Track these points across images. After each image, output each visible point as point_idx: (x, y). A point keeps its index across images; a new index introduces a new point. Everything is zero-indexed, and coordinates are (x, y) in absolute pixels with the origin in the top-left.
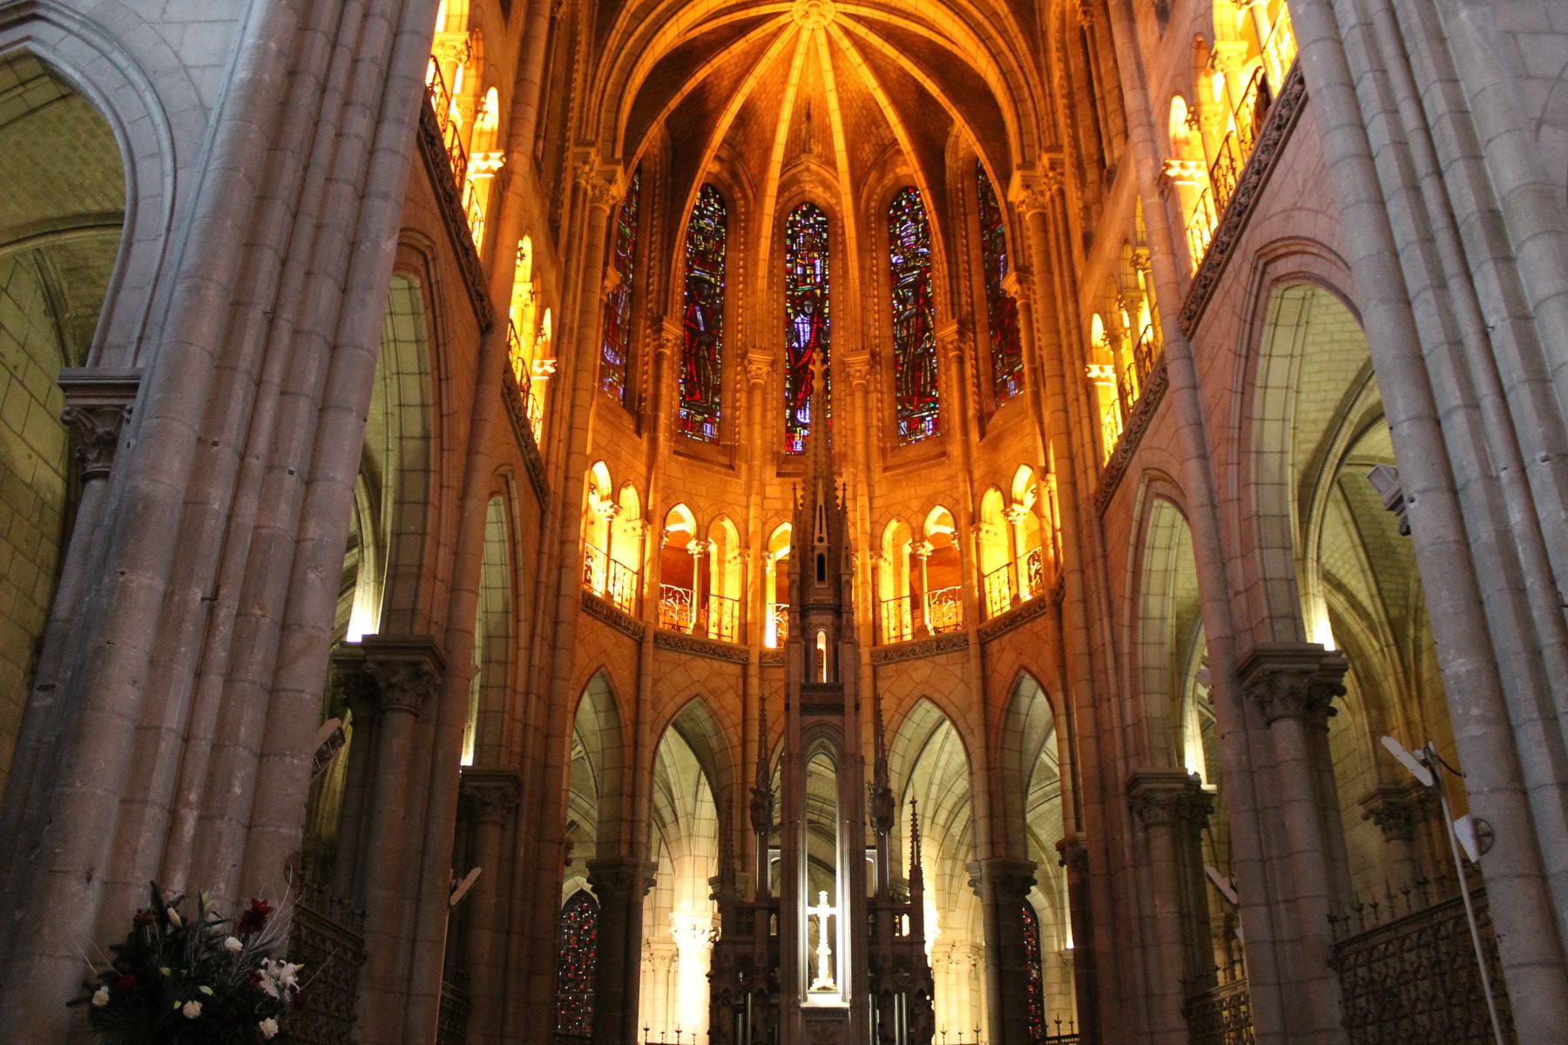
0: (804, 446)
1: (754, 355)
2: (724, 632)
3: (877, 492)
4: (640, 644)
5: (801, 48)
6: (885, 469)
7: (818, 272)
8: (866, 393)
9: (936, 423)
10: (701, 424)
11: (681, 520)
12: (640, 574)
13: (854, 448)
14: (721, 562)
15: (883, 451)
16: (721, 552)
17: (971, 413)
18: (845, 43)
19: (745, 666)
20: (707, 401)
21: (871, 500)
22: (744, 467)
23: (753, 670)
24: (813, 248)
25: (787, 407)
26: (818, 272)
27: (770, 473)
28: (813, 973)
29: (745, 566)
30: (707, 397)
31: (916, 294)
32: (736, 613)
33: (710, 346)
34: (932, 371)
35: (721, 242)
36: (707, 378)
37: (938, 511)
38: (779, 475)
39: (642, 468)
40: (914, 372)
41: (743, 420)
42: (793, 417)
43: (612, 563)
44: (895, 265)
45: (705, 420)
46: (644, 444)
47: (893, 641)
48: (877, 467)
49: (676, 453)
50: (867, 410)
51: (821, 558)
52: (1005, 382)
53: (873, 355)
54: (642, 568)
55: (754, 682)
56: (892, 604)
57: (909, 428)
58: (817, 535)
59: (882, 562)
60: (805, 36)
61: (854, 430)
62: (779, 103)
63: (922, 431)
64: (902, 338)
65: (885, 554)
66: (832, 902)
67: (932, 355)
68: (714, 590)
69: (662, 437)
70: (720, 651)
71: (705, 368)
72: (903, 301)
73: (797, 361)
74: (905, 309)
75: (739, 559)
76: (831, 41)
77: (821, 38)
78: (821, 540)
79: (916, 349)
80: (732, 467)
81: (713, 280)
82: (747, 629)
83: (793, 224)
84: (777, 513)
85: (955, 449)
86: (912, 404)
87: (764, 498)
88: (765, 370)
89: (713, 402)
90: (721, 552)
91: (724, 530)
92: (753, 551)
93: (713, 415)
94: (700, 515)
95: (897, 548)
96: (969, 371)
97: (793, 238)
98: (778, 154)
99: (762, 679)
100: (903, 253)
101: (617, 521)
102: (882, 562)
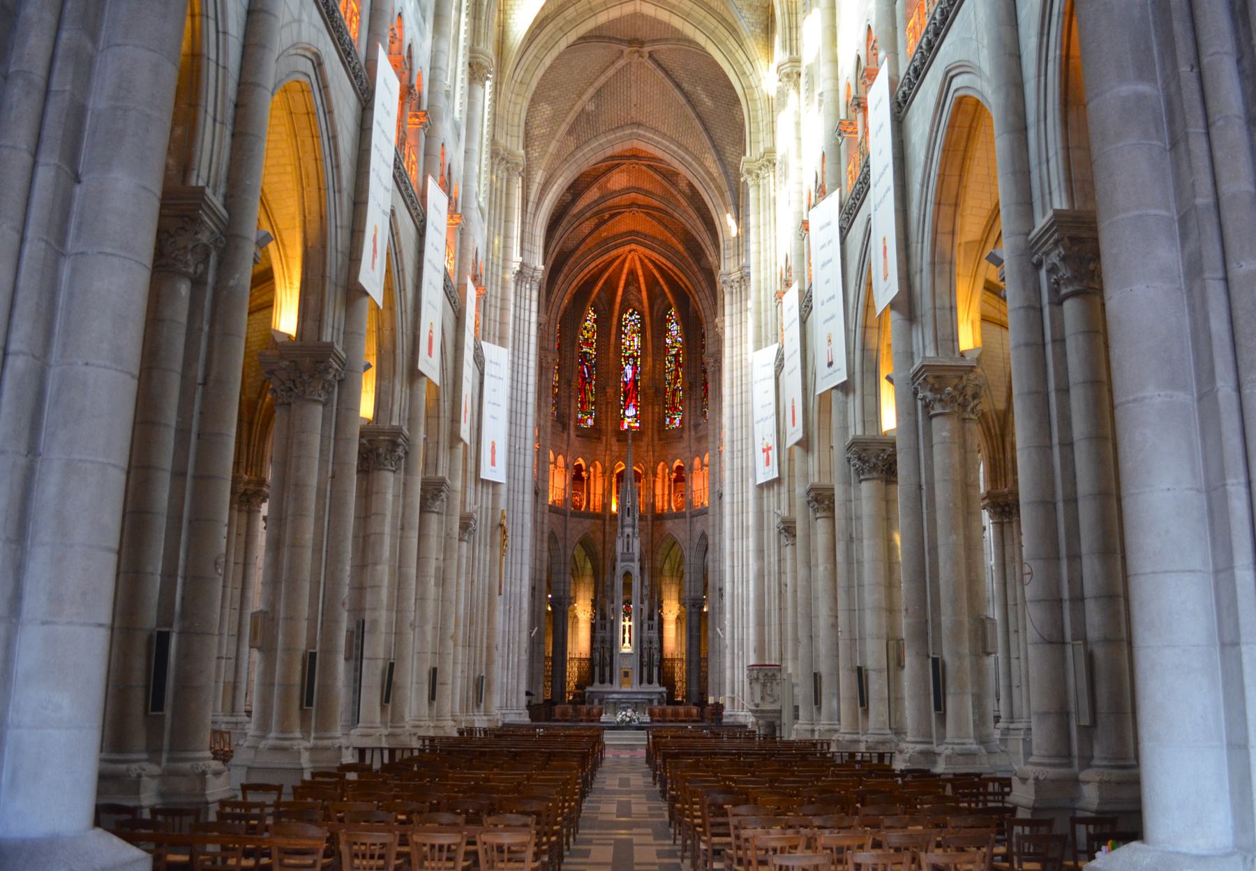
3: (656, 449)
4: (565, 515)
8: (653, 405)
9: (681, 422)
12: (565, 489)
14: (595, 476)
15: (659, 432)
16: (595, 471)
18: (646, 261)
19: (604, 520)
21: (654, 452)
22: (604, 438)
23: (607, 522)
24: (634, 332)
27: (614, 440)
28: (624, 642)
33: (590, 383)
38: (618, 441)
39: (565, 447)
41: (604, 417)
48: (656, 438)
49: (578, 436)
50: (653, 413)
55: (607, 527)
60: (630, 257)
62: (619, 279)
66: (630, 620)
68: (592, 491)
69: (572, 432)
70: (596, 516)
72: (670, 362)
77: (637, 258)
82: (606, 505)
83: (626, 319)
85: (686, 435)
87: (612, 451)
90: (595, 471)
95: (663, 470)
96: (693, 404)
97: (625, 326)
98: (618, 299)
99: (610, 525)
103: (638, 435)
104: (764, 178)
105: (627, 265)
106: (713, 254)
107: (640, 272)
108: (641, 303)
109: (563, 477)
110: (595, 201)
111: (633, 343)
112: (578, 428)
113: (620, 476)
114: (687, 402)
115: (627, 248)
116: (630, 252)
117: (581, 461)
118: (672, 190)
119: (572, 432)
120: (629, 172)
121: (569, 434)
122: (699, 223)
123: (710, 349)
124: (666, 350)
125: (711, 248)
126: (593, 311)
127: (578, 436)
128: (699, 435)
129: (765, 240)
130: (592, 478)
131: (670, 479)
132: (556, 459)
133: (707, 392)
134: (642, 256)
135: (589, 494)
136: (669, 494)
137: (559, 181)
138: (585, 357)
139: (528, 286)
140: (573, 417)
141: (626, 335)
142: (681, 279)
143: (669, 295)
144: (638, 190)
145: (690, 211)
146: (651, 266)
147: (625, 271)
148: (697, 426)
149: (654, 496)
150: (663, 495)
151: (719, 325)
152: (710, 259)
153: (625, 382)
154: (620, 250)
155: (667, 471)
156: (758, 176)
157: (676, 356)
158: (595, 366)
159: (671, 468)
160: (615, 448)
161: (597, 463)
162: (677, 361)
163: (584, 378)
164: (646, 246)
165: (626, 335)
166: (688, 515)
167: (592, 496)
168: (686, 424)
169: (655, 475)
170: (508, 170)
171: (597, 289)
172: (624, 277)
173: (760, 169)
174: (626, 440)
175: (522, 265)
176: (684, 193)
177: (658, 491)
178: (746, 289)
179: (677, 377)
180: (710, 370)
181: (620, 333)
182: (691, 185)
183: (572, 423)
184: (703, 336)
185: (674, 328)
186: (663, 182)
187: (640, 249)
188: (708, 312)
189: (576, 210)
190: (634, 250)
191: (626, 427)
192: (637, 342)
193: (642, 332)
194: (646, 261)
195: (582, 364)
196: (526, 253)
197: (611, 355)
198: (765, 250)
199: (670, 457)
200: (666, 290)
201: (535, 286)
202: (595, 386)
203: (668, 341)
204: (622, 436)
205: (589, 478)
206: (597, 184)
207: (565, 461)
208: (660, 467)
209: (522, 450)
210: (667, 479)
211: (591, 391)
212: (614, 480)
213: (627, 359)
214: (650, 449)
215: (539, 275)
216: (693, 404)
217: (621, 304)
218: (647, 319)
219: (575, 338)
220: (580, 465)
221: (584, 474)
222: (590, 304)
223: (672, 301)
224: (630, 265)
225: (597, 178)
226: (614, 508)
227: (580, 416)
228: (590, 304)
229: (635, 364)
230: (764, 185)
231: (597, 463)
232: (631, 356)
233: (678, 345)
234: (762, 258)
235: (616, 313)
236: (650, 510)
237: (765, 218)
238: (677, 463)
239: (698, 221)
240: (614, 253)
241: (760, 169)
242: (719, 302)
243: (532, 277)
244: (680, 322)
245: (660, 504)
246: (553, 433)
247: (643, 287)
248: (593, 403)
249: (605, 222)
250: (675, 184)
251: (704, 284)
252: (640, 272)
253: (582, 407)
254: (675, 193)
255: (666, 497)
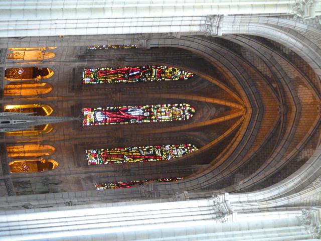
0: (86, 115)
1: (119, 95)
2: (8, 91)
3: (67, 143)
5: (237, 106)
6: (76, 145)
7: (163, 117)
9: (93, 164)
10: (90, 77)
11: (51, 72)
12: (23, 61)
13: (85, 134)
14: (38, 87)
15: (83, 144)
17: (93, 174)
18: (238, 123)
20: (100, 78)
21: (64, 140)
22: (73, 94)
25: (102, 109)
26: (163, 117)
27: (72, 103)
29: (35, 96)
30: (102, 78)
31: (150, 155)
32: (16, 95)
33: (124, 78)
34: (115, 161)
35: (171, 78)
36: (109, 78)
37: (57, 164)
38: (72, 107)
40: (116, 155)
42: (98, 111)
43: (23, 52)
44: (165, 147)
45: (91, 78)
46: (72, 59)
47: (8, 150)
48: (76, 142)
51: (9, 122)
52: (104, 186)
53: (122, 139)
54: (27, 61)
56: (23, 149)
57: (93, 153)
58: (16, 121)
59: (39, 145)
60: (241, 107)
61: (92, 134)
62: (221, 99)
63: (91, 158)
64: (131, 150)
65: (42, 146)
67: (122, 161)
68: (24, 86)
69: (77, 64)
71: (114, 77)
72: (148, 150)
73: (123, 111)
74: (144, 151)
75: (36, 94)
76: (241, 116)
77: (241, 114)
78: (15, 122)
79: (126, 155)
80: (73, 89)
81: (153, 77)
84: (56, 107)
85: (81, 169)
86: (103, 154)
87: (62, 101)
88: (114, 99)
89: (100, 81)
91: (49, 88)
92: (40, 99)
93: (94, 81)
94: (51, 79)
95: (48, 151)
96: (110, 174)
97: (178, 107)
100: (170, 150)
101: (39, 52)
102: (39, 145)
103: (79, 125)
104: (306, 229)
105: (233, 105)
106: (245, 185)
107: (228, 118)
108: (201, 119)
109: (35, 58)
110: (286, 75)
111: (164, 114)
112: (81, 69)
113: (39, 112)
114: (112, 169)
115: (248, 105)
116: (245, 107)
117: (51, 74)
118: (300, 144)
119: (77, 64)
120: (314, 103)
121: (75, 61)
122: (271, 171)
123: (162, 187)
124: (160, 145)
125: (251, 182)
126: (190, 78)
127: (74, 69)
128: (83, 182)
129: (251, 234)
130: (36, 85)
131: (39, 157)
132: (51, 51)
133: (123, 186)
134: (242, 118)
135: (21, 83)
136: (24, 158)
137: (299, 45)
138: (148, 72)
139: (203, 22)
140: (91, 64)
141: (171, 107)
142: (223, 155)
143: (208, 146)
144: (299, 113)
145: (283, 161)
146: (234, 127)
147: (228, 104)
148: (90, 179)
149: (23, 144)
150: (24, 152)
151: (182, 195)
152: (241, 183)
153: (125, 111)
154: (245, 98)
155: (47, 154)
156: (309, 224)
157: (154, 155)
158: (139, 80)
159: (50, 157)
160: (66, 105)
161: (50, 89)
162: (149, 156)
163: (127, 72)
164: (250, 122)
165: (171, 107)
166: (6, 177)
167: (19, 86)
168: (91, 169)
169: (43, 143)
170: (297, 4)
171: (209, 78)
172: (223, 103)
173: (314, 225)
174: (73, 115)
175: (221, 17)
176: (298, 155)
177: (27, 148)
178: (213, 218)
179: (134, 159)
180: (143, 188)
181: (172, 102)
182: (304, 161)
183: (85, 64)
184: (174, 179)
185: (179, 152)
186: (307, 135)
187: (248, 117)
188: (194, 183)
189: (277, 57)
190: (247, 112)
191: (85, 113)
192: (165, 118)
193: (174, 122)
194: (238, 123)
195: (141, 69)
196: (232, 19)
197: (151, 96)
198: (242, 235)
199: (60, 156)
200: (213, 143)
201: (203, 29)
202: (122, 83)
203: (167, 146)
204: (76, 111)
205: (36, 82)
206: (301, 76)
207: (49, 60)
208: (50, 147)
209: (54, 26)
210: (39, 154)
211: (117, 80)
212: (36, 106)
213: (149, 110)
214: (67, 137)
215: (214, 32)
216: (110, 174)
217: (199, 102)
218: (186, 127)
219: (164, 62)
220: (47, 74)
221: (39, 77)
222: (196, 73)
223: (203, 149)
224: (234, 108)
225: (306, 75)
226: (9, 107)
227: (93, 70)
228: (196, 73)
229: (145, 118)
230: (300, 230)
231: (50, 89)
232: (151, 114)
233: (164, 157)
234: (235, 233)
235: (189, 98)
236: (10, 141)
237: (271, 232)
238: (55, 163)
239: (274, 169)
240: (243, 93)
241: (314, 225)
242: (202, 194)
243: (211, 26)
244: (185, 157)
245: (15, 150)
246: (75, 48)
247: (215, 121)
248: (105, 81)
249: (270, 84)
250: (305, 146)
251: (219, 177)
252: (228, 118)
253: (101, 72)
254: (298, 147)
255: (23, 155)
